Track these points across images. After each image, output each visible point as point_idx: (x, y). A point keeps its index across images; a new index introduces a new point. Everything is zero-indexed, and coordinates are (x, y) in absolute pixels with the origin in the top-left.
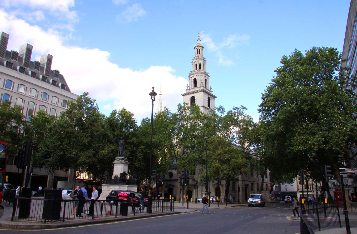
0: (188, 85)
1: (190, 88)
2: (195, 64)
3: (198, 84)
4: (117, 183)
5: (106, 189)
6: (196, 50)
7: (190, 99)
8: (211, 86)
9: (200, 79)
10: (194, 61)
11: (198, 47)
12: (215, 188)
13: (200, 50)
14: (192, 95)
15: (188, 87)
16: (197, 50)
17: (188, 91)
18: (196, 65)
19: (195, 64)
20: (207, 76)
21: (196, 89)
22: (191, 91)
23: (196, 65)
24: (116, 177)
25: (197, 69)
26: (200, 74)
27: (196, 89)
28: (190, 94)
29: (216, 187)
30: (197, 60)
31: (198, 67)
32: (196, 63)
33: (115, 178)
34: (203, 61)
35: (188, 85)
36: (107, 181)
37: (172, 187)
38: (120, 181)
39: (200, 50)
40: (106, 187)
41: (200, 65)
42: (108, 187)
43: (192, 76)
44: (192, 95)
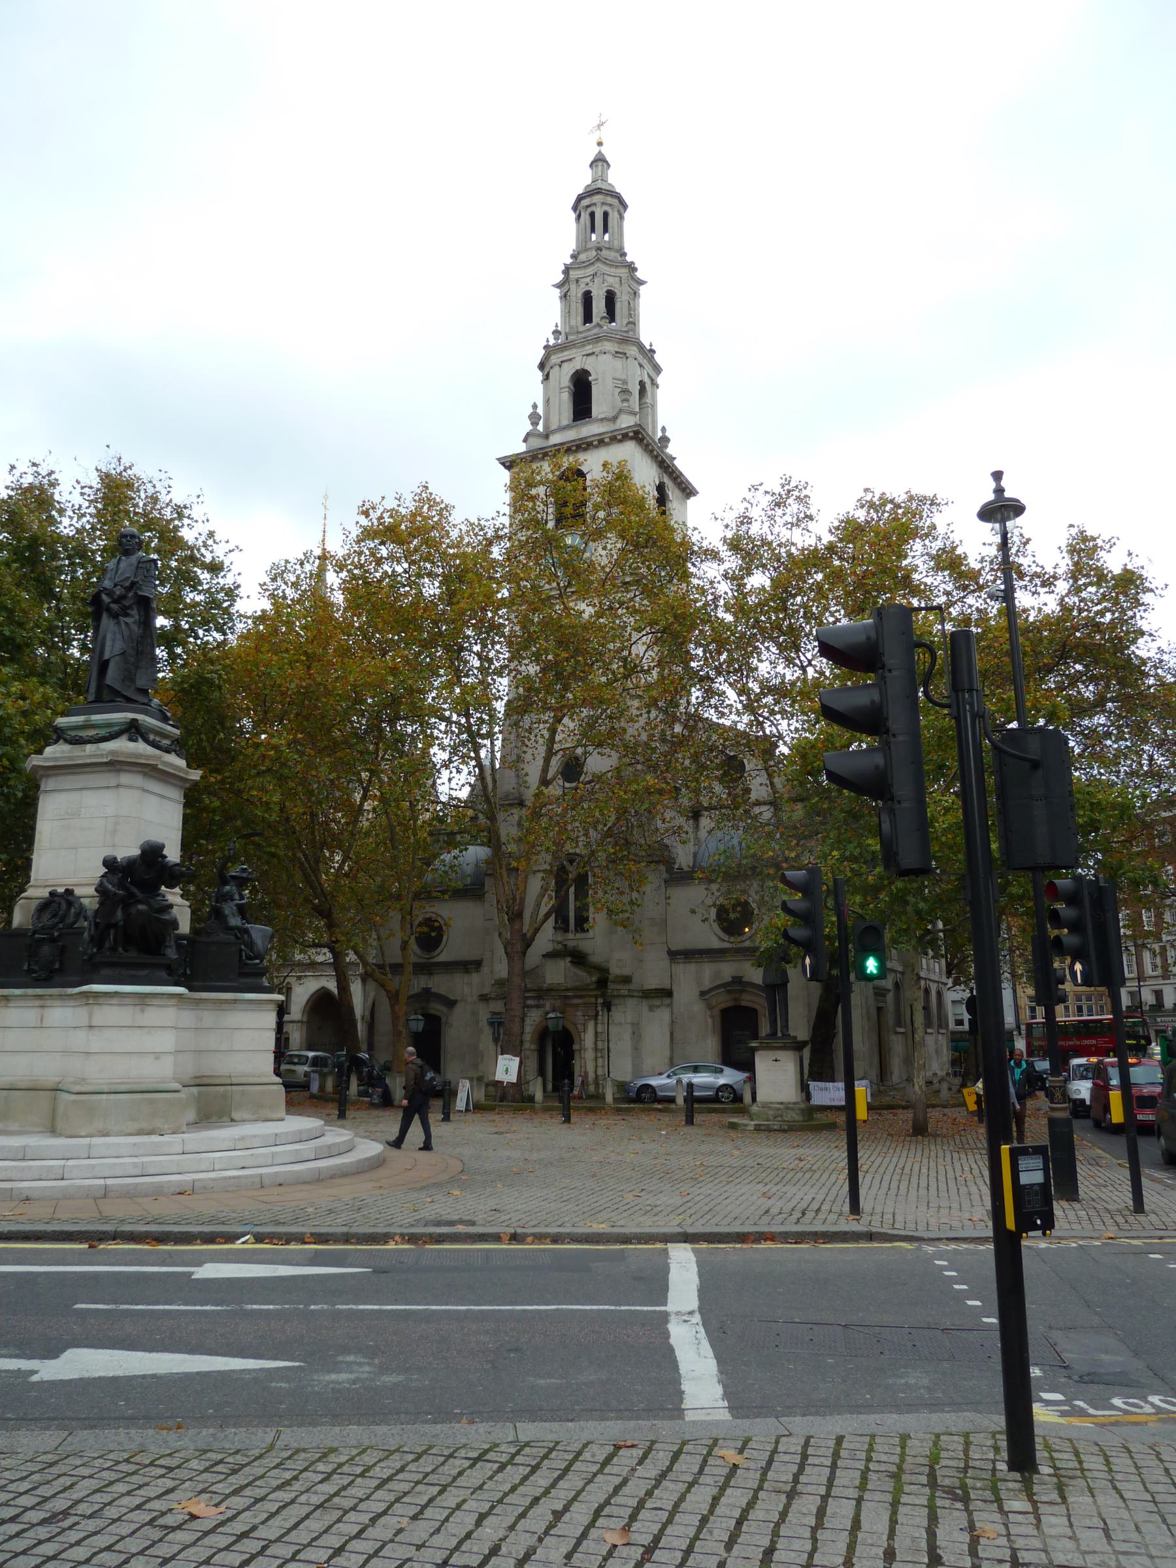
0: (535, 406)
1: (554, 427)
2: (577, 293)
3: (599, 407)
6: (585, 216)
8: (664, 429)
9: (606, 372)
10: (574, 274)
11: (597, 198)
12: (717, 1012)
13: (606, 215)
15: (534, 418)
16: (592, 215)
17: (537, 443)
18: (587, 299)
19: (580, 295)
20: (648, 368)
21: (589, 430)
22: (555, 439)
23: (587, 299)
24: (60, 903)
25: (596, 319)
26: (609, 346)
27: (589, 430)
29: (723, 1006)
30: (590, 271)
31: (599, 307)
32: (583, 288)
33: (46, 918)
34: (624, 276)
35: (535, 406)
37: (436, 1008)
38: (98, 940)
39: (606, 215)
41: (610, 299)
43: (566, 355)
44: (567, 461)
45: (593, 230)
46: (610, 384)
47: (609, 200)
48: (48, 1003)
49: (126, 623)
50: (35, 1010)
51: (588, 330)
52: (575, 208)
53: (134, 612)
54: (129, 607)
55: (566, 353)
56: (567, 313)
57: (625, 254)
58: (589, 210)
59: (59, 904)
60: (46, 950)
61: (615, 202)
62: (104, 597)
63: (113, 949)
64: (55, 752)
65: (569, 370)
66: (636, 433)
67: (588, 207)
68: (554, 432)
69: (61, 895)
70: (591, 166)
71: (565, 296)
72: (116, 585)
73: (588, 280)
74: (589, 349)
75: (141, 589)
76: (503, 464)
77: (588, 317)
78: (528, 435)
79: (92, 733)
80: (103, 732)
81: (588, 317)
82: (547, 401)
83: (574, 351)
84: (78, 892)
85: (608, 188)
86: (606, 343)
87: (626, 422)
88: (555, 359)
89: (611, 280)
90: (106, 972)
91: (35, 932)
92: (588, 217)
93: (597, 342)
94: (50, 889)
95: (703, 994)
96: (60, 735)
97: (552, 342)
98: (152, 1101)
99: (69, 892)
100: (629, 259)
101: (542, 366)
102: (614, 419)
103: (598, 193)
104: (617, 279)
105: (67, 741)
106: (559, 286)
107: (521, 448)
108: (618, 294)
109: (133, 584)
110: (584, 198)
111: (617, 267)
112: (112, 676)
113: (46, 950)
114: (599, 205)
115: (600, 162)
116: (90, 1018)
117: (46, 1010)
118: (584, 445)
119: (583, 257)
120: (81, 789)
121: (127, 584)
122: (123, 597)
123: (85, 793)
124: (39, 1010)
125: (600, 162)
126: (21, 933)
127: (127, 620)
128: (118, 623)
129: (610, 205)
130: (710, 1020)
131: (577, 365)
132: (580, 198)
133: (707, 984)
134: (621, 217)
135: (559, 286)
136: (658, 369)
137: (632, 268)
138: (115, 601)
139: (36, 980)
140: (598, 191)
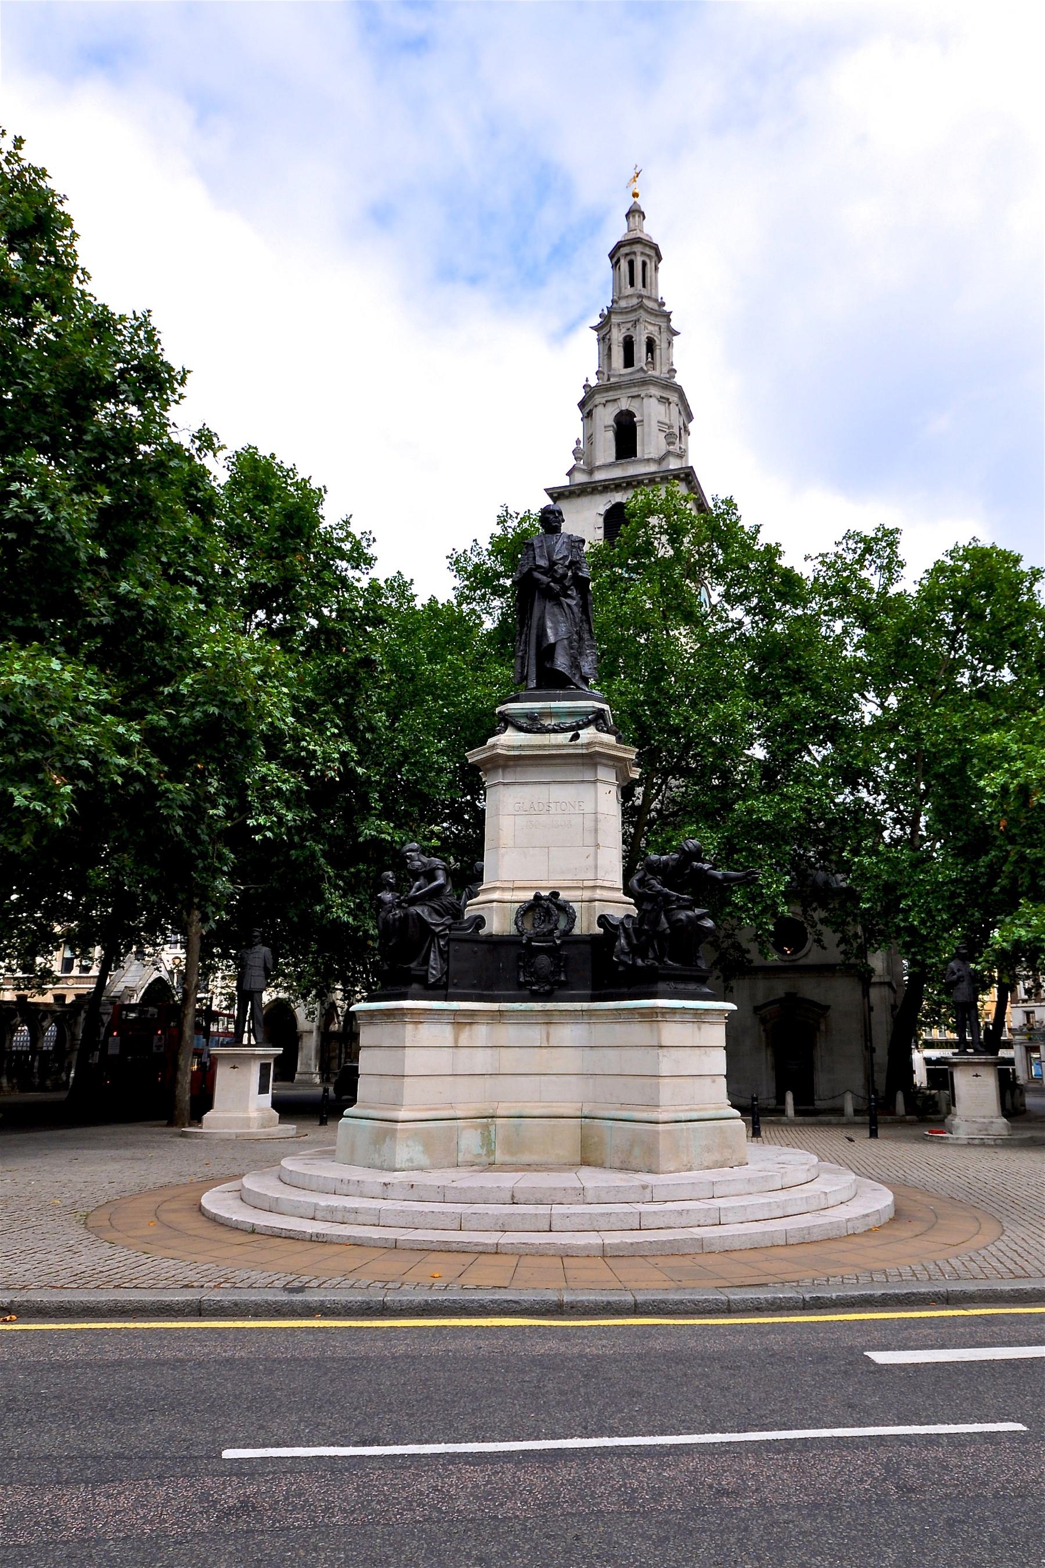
2: (617, 337)
4: (563, 985)
5: (442, 1061)
6: (624, 265)
7: (601, 520)
10: (615, 319)
11: (638, 248)
13: (644, 264)
16: (631, 264)
17: (580, 478)
18: (628, 345)
19: (621, 339)
22: (600, 476)
23: (628, 345)
24: (545, 908)
30: (632, 317)
34: (664, 325)
35: (578, 442)
36: (443, 955)
40: (441, 1033)
42: (464, 1038)
43: (611, 395)
46: (655, 426)
47: (648, 251)
49: (569, 606)
50: (539, 1027)
51: (631, 374)
52: (611, 256)
53: (573, 592)
54: (568, 588)
55: (611, 393)
56: (606, 353)
57: (663, 304)
58: (629, 258)
59: (548, 909)
60: (543, 961)
61: (652, 253)
62: (537, 575)
64: (509, 739)
66: (688, 475)
67: (627, 255)
68: (599, 468)
69: (547, 899)
70: (627, 216)
71: (604, 338)
72: (553, 563)
73: (629, 325)
74: (634, 391)
75: (580, 569)
78: (574, 468)
81: (629, 362)
82: (589, 438)
83: (619, 392)
84: (563, 895)
85: (647, 238)
86: (651, 387)
87: (674, 464)
88: (599, 399)
89: (650, 328)
90: (662, 986)
91: (530, 940)
92: (627, 264)
93: (643, 385)
94: (533, 893)
95: (756, 1009)
96: (508, 721)
97: (594, 382)
98: (695, 1130)
99: (555, 895)
100: (667, 308)
101: (582, 405)
103: (638, 242)
104: (657, 328)
105: (520, 729)
106: (596, 328)
107: (565, 481)
108: (658, 342)
110: (624, 246)
111: (656, 315)
114: (638, 254)
115: (635, 213)
117: (552, 1026)
118: (617, 485)
119: (623, 304)
120: (549, 783)
121: (567, 563)
122: (565, 576)
123: (553, 787)
124: (544, 1027)
125: (635, 213)
126: (496, 943)
127: (569, 601)
128: (560, 604)
129: (648, 256)
130: (763, 1034)
131: (624, 404)
132: (619, 246)
133: (761, 1000)
134: (656, 268)
135: (596, 328)
136: (690, 417)
137: (667, 316)
140: (638, 241)
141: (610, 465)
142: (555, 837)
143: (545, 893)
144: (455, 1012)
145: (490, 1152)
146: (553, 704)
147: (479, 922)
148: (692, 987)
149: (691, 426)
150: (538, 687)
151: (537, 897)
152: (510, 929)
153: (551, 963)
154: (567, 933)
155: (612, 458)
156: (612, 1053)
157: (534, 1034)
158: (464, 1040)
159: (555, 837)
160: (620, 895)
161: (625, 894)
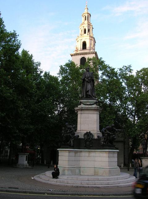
14: (83, 56)
16: (86, 17)
18: (85, 30)
24: (88, 134)
28: (81, 54)
33: (86, 136)
45: (86, 20)
48: (90, 152)
63: (108, 143)
64: (82, 106)
65: (82, 41)
76: (71, 55)
77: (85, 33)
79: (88, 103)
80: (92, 103)
81: (85, 33)
84: (91, 132)
102: (90, 50)
109: (92, 77)
112: (89, 93)
113: (88, 143)
116: (89, 155)
117: (90, 154)
118: (83, 54)
123: (89, 114)
138: (89, 80)
139: (87, 148)
141: (82, 50)
142: (88, 122)
143: (88, 132)
144: (75, 151)
145: (80, 173)
146: (89, 100)
147: (78, 136)
148: (112, 148)
149: (95, 44)
150: (86, 97)
151: (87, 132)
152: (83, 137)
153: (88, 143)
154: (92, 139)
155: (82, 49)
156: (100, 158)
157: (87, 154)
158: (76, 155)
159: (88, 122)
160: (100, 132)
161: (100, 132)
